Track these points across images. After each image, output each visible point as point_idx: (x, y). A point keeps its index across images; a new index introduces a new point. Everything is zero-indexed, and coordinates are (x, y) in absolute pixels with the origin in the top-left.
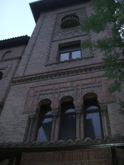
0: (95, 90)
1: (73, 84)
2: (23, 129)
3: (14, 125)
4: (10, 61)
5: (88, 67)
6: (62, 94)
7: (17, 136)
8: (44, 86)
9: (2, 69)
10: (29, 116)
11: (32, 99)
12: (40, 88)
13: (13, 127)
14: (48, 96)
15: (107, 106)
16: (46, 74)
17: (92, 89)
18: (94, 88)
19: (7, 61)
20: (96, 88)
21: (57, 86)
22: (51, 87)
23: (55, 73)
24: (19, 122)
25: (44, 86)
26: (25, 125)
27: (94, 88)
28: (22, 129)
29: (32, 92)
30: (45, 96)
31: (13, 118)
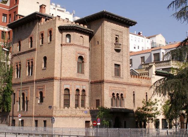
19: (83, 48)
21: (116, 88)
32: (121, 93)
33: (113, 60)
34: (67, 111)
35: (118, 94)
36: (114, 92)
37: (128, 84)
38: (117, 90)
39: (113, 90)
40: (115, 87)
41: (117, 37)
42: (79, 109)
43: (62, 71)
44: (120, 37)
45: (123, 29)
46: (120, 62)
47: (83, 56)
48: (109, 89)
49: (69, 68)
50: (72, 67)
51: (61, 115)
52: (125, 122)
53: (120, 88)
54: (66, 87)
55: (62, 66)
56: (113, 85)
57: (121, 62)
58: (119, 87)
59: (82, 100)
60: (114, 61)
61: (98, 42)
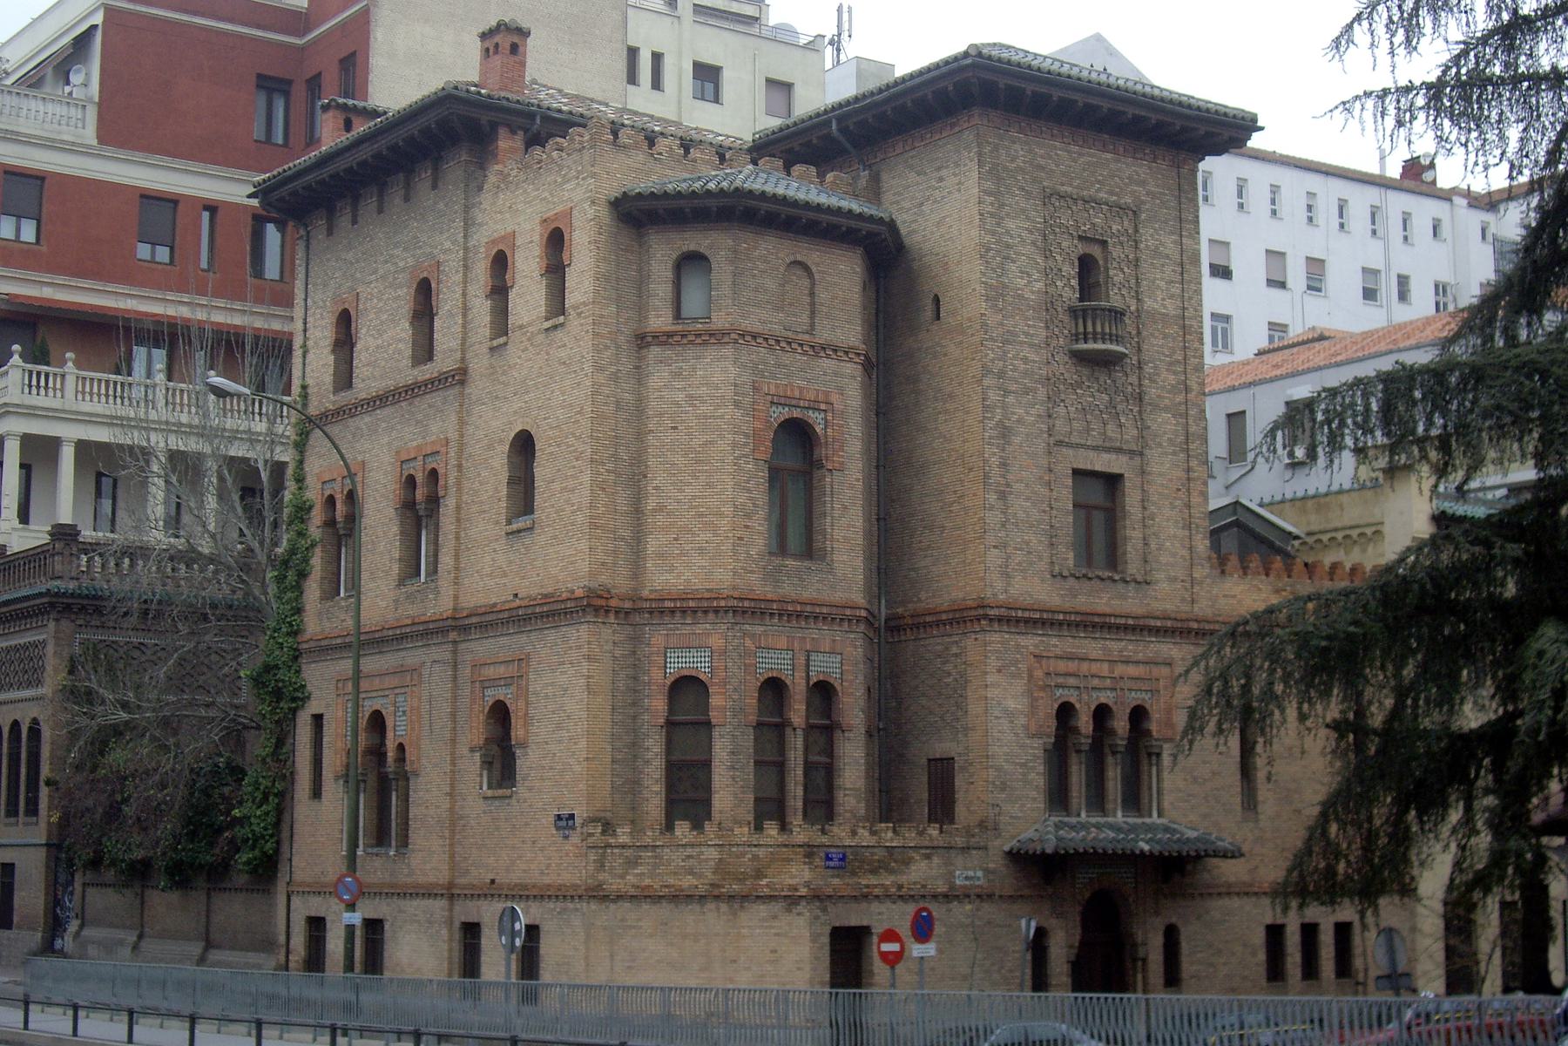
4: (828, 356)
5: (1141, 622)
16: (1061, 617)
19: (817, 355)
21: (1085, 667)
22: (1072, 666)
29: (1039, 673)
32: (1134, 698)
33: (1059, 443)
34: (689, 851)
35: (1102, 714)
37: (1189, 631)
38: (1096, 682)
39: (1060, 680)
41: (1096, 251)
42: (782, 839)
43: (652, 544)
44: (1116, 252)
45: (1143, 183)
46: (1119, 450)
47: (815, 418)
48: (1030, 676)
49: (701, 515)
50: (727, 509)
51: (647, 882)
52: (1171, 936)
54: (680, 663)
55: (651, 504)
56: (1058, 643)
57: (1132, 452)
59: (809, 767)
60: (1071, 452)
61: (937, 300)
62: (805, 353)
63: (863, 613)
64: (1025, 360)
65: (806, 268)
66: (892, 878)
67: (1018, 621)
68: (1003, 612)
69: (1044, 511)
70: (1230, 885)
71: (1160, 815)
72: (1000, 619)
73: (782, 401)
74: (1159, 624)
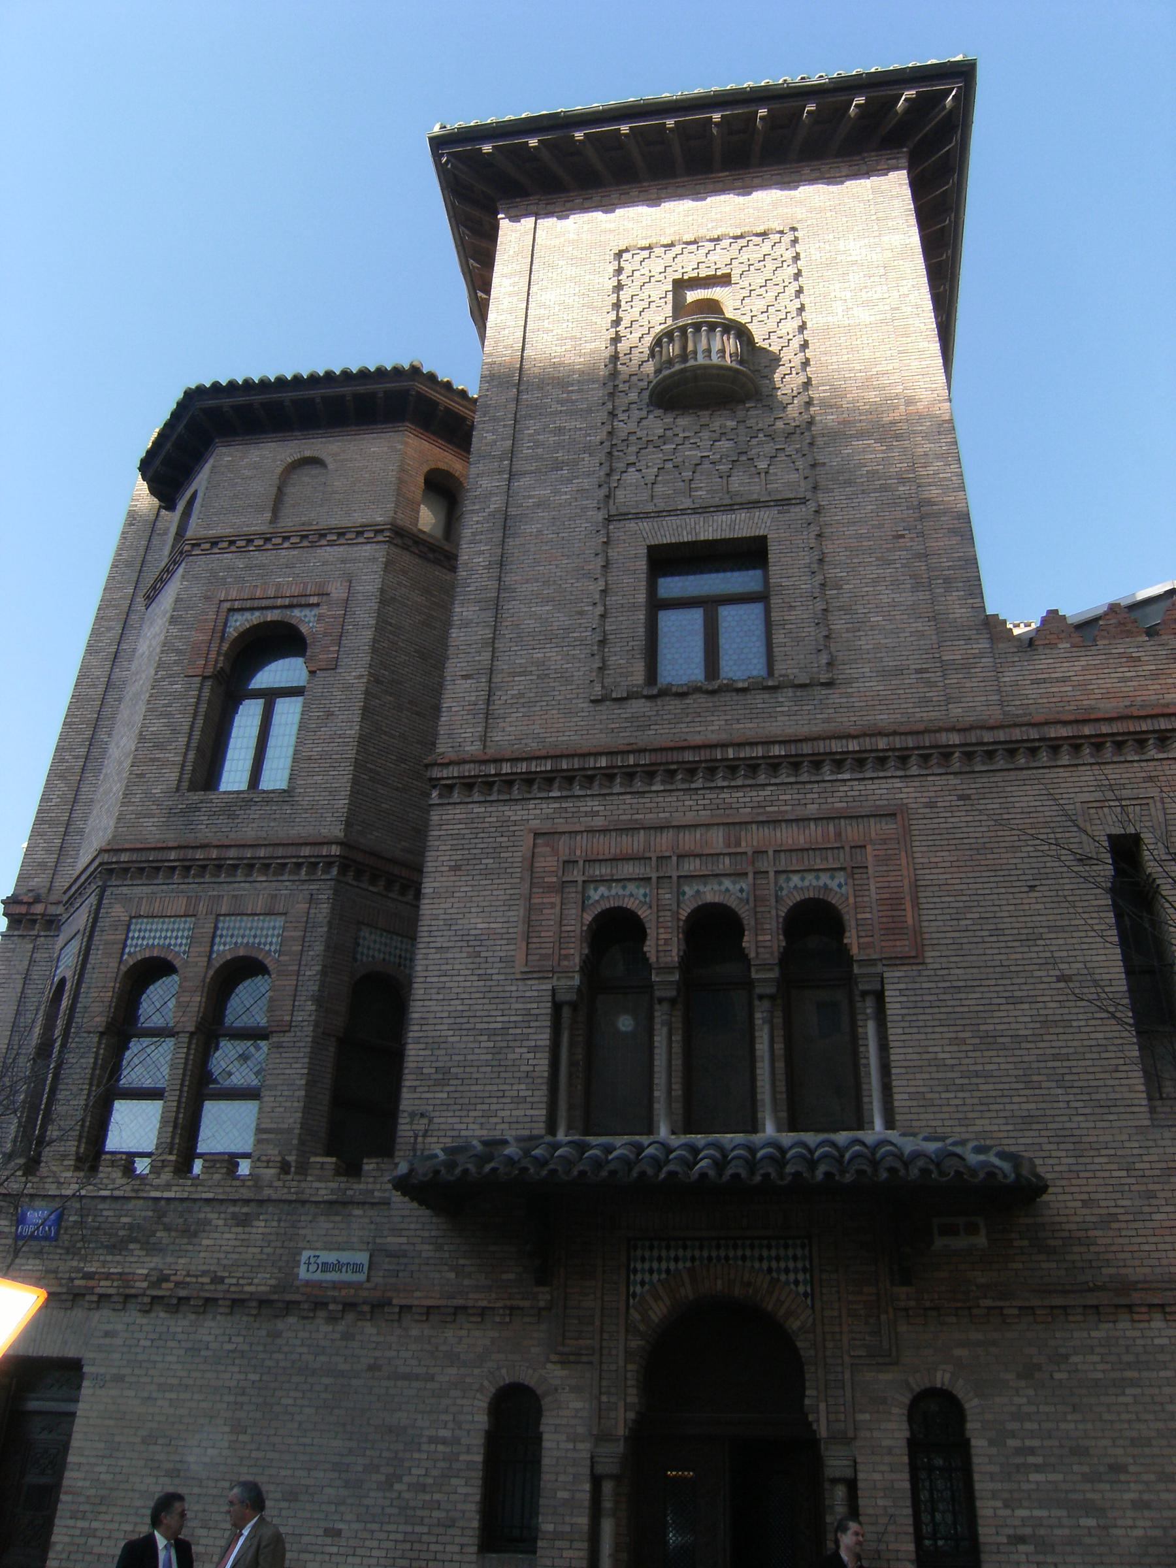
0: (833, 884)
1: (738, 844)
2: (538, 1055)
3: (492, 1033)
4: (331, 544)
5: (806, 749)
6: (689, 890)
7: (515, 1087)
8: (604, 831)
9: (295, 601)
10: (553, 990)
11: (553, 900)
12: (582, 841)
13: (491, 1044)
14: (627, 892)
15: (882, 978)
16: (603, 762)
17: (824, 879)
18: (832, 878)
19: (313, 545)
20: (841, 877)
21: (663, 842)
22: (635, 843)
23: (645, 759)
24: (513, 1019)
25: (604, 831)
26: (544, 1038)
27: (832, 878)
28: (531, 1055)
29: (547, 863)
30: (613, 892)
31: (481, 995)
36: (633, 898)
38: (692, 866)
40: (661, 828)
53: (775, 822)
58: (745, 813)
60: (645, 525)
62: (294, 547)
63: (335, 850)
64: (560, 431)
65: (315, 461)
66: (155, 1261)
67: (508, 783)
68: (469, 770)
69: (581, 613)
70: (1125, 1287)
71: (890, 1124)
72: (469, 785)
73: (248, 604)
74: (853, 746)
